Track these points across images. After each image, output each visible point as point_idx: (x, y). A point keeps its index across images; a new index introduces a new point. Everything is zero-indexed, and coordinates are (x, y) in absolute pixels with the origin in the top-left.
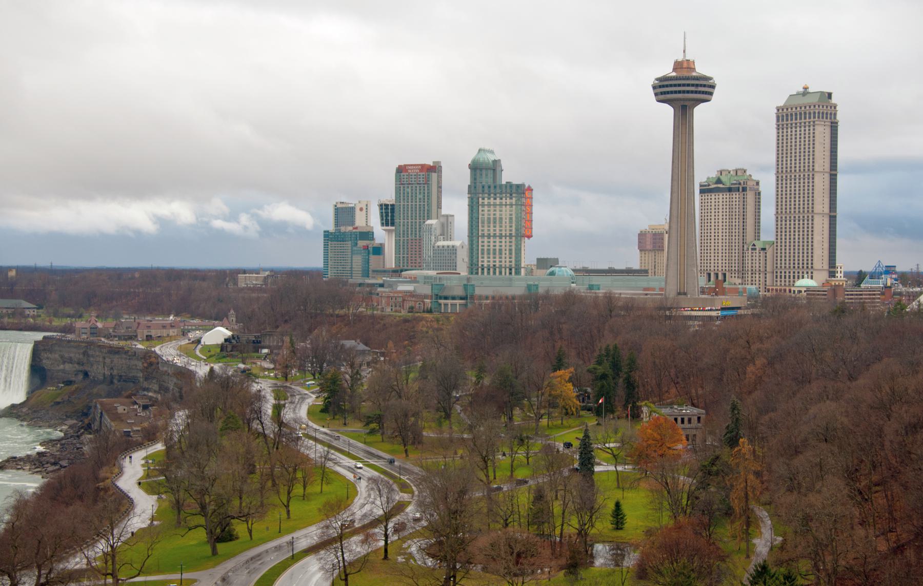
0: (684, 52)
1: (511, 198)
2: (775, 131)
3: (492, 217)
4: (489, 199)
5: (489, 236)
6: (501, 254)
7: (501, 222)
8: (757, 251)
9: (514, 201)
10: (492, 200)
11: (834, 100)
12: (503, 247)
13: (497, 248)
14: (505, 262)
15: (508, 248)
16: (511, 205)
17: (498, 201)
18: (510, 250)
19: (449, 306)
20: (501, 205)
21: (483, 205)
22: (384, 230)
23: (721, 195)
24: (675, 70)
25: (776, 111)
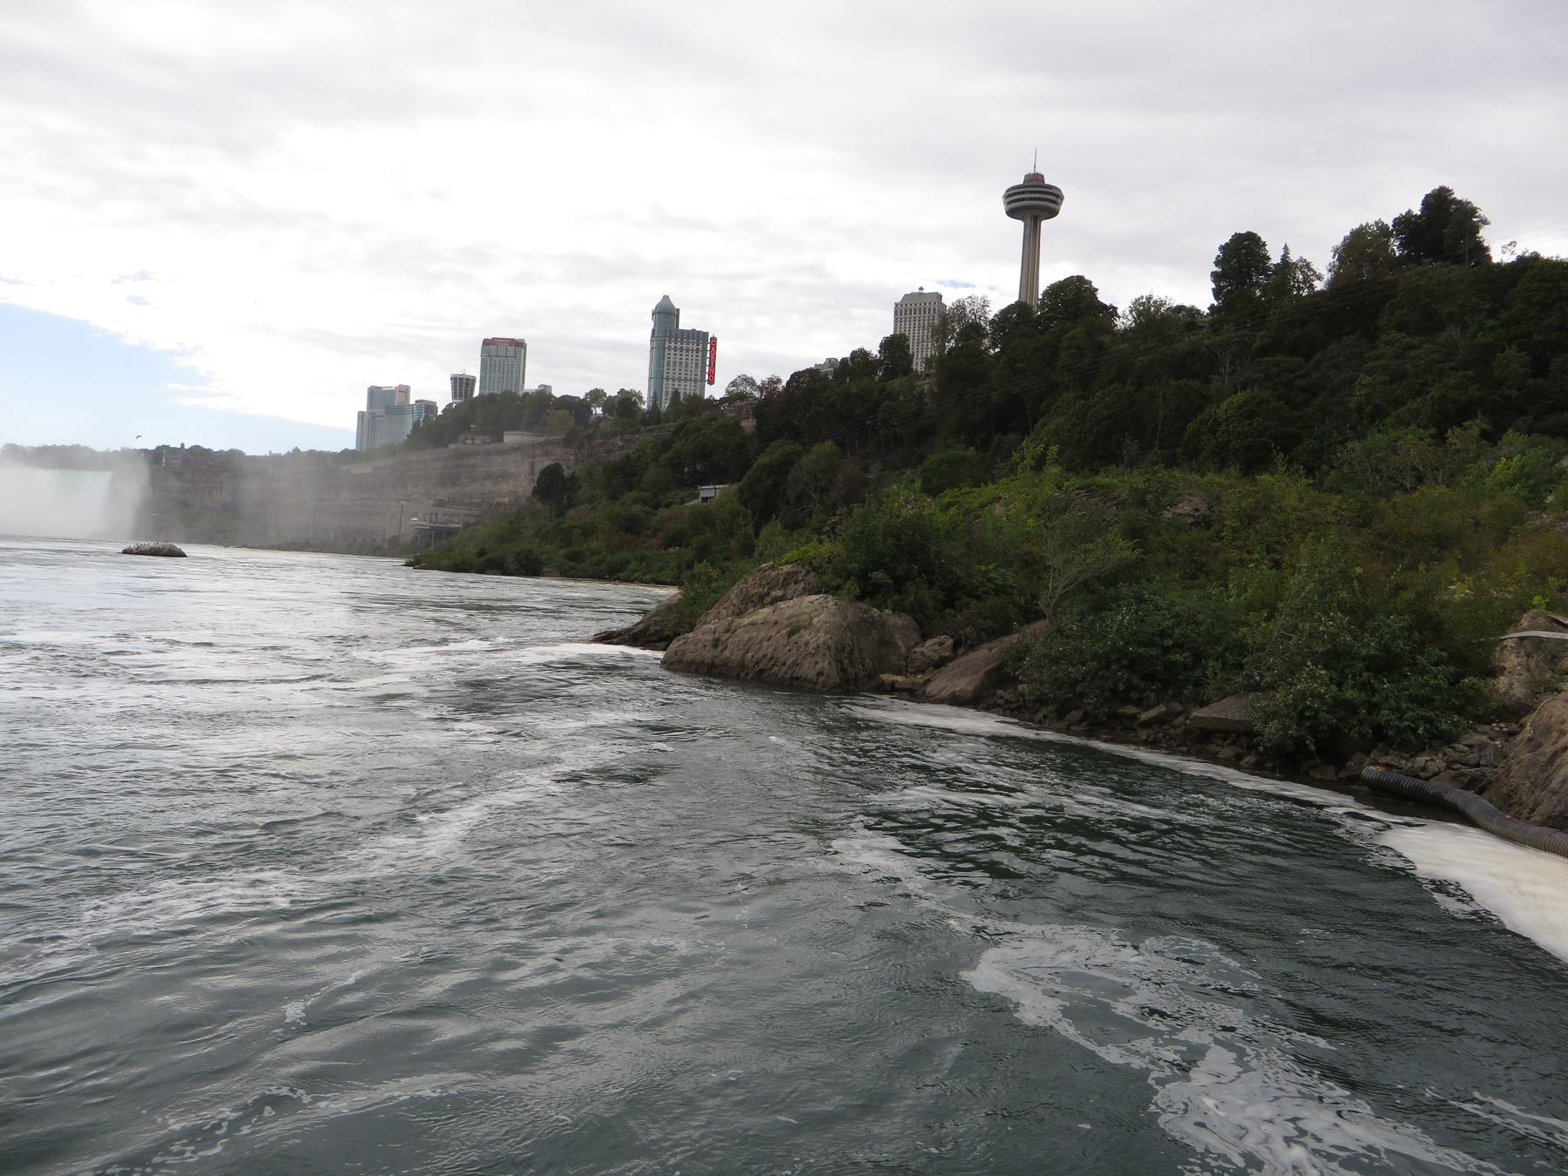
7: (687, 366)
9: (700, 347)
10: (679, 345)
16: (697, 352)
17: (685, 346)
21: (669, 348)
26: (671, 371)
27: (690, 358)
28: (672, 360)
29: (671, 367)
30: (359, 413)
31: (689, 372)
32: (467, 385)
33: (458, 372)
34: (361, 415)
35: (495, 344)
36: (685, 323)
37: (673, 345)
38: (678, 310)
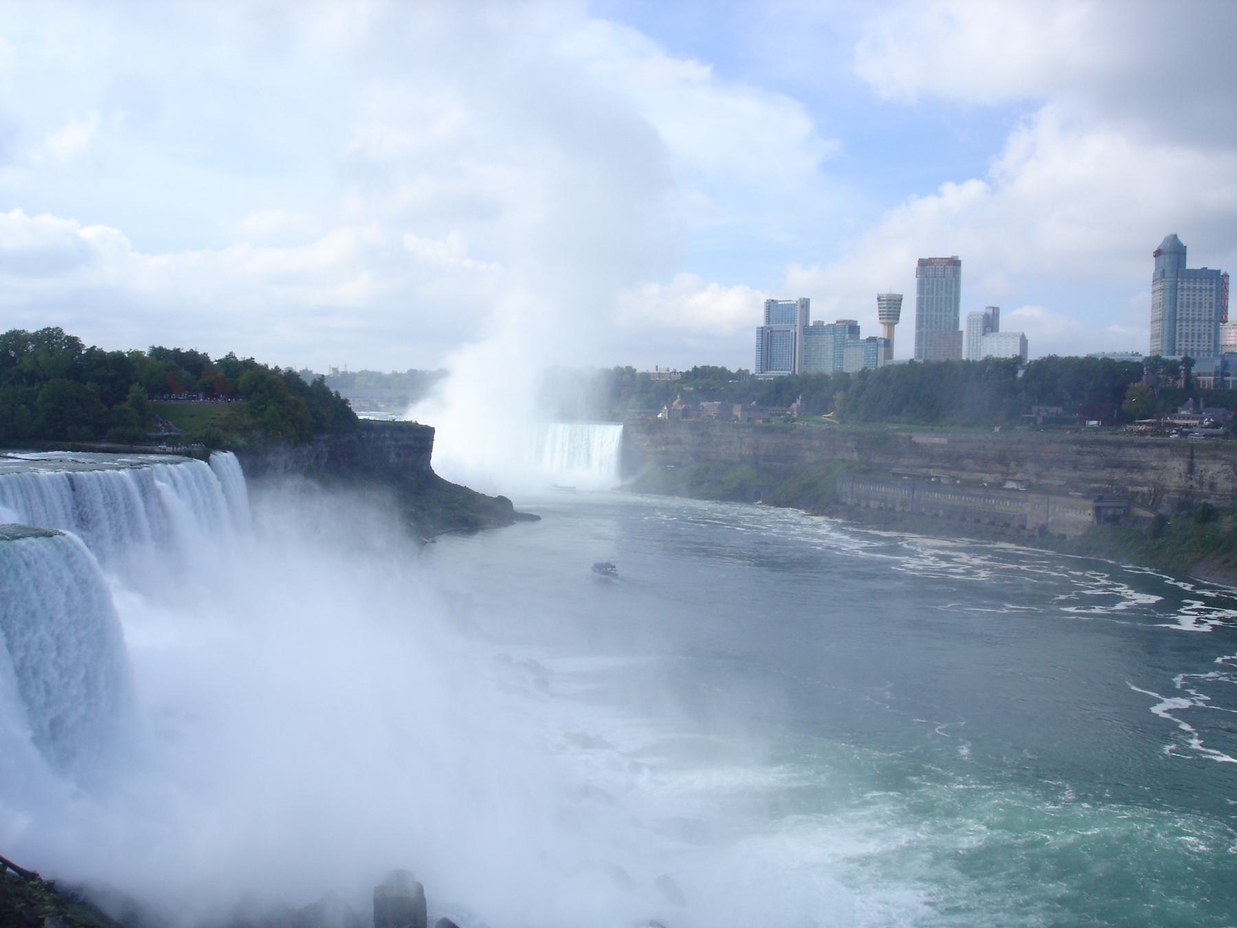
1: (1211, 284)
3: (1191, 301)
4: (1189, 282)
6: (1199, 337)
7: (1200, 307)
9: (1214, 286)
10: (1192, 285)
12: (1202, 331)
13: (1196, 332)
14: (1204, 346)
15: (1207, 332)
16: (1211, 290)
17: (1198, 286)
18: (1209, 334)
19: (1231, 383)
20: (1201, 288)
21: (1182, 289)
22: (883, 323)
26: (1184, 312)
27: (1203, 297)
28: (1185, 300)
29: (1185, 308)
30: (757, 328)
31: (1203, 313)
35: (932, 264)
36: (1192, 264)
37: (1185, 285)
38: (1186, 247)
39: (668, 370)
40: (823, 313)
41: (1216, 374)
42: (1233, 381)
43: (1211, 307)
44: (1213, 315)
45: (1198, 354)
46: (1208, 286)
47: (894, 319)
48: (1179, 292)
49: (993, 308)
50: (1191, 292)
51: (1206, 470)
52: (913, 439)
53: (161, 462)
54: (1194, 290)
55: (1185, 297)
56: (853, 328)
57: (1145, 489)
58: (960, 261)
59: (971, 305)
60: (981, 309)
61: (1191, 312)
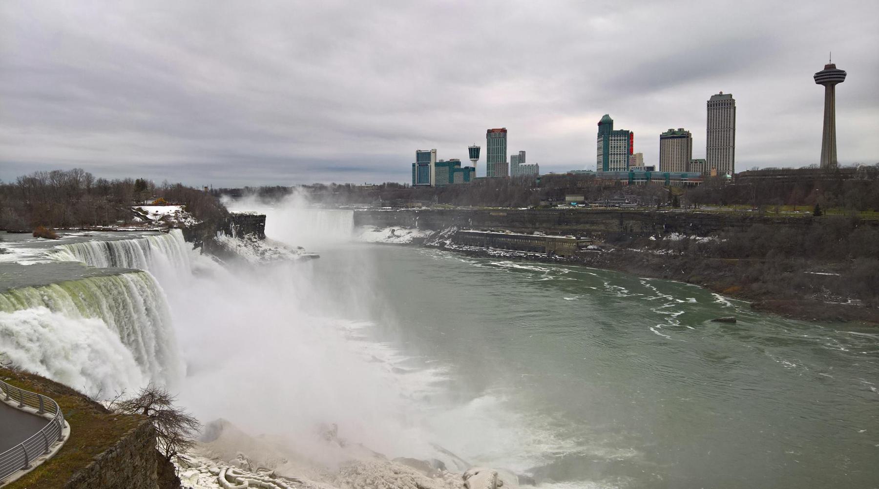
0: (830, 60)
2: (706, 111)
5: (614, 154)
8: (698, 163)
9: (626, 138)
11: (733, 98)
13: (618, 160)
15: (623, 160)
16: (625, 140)
17: (619, 138)
18: (625, 161)
20: (620, 140)
21: (612, 140)
23: (675, 140)
24: (825, 69)
25: (707, 102)
28: (613, 145)
32: (477, 150)
33: (472, 145)
34: (414, 165)
35: (494, 132)
36: (616, 127)
37: (613, 138)
39: (371, 184)
40: (444, 154)
41: (629, 179)
42: (637, 182)
43: (625, 148)
44: (626, 150)
45: (620, 170)
46: (624, 138)
47: (477, 158)
48: (610, 142)
49: (523, 152)
50: (616, 141)
51: (629, 224)
52: (491, 214)
53: (149, 235)
54: (617, 140)
55: (613, 143)
56: (458, 163)
57: (600, 233)
58: (506, 130)
59: (512, 150)
60: (517, 153)
61: (616, 150)
